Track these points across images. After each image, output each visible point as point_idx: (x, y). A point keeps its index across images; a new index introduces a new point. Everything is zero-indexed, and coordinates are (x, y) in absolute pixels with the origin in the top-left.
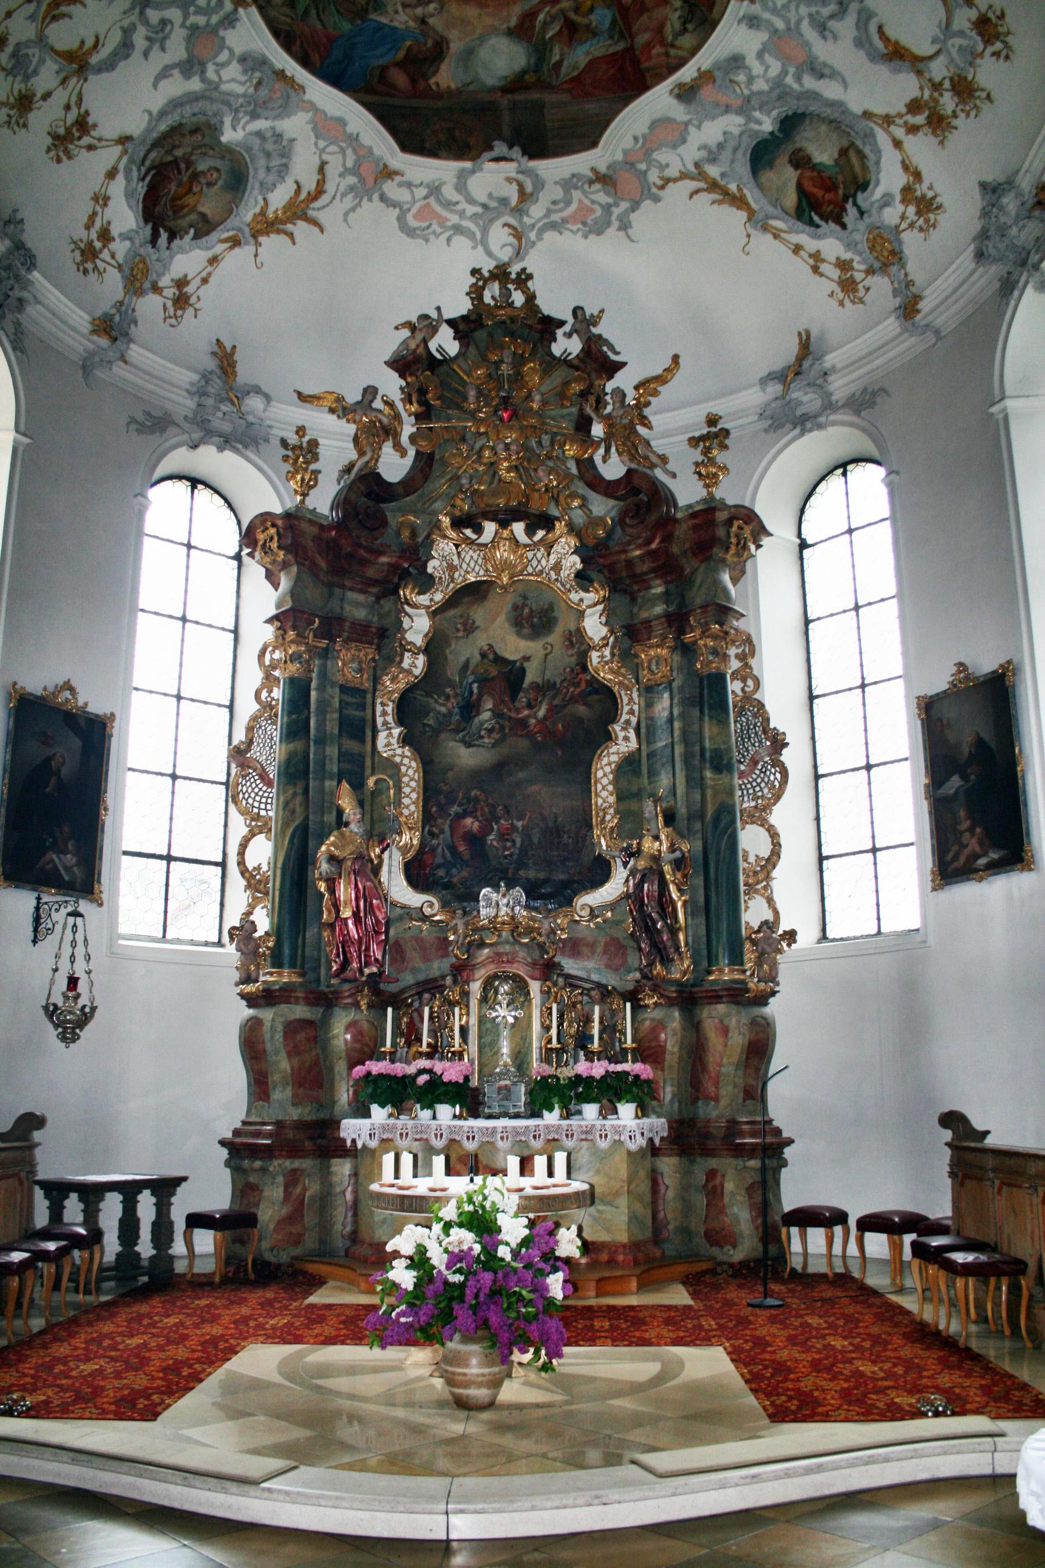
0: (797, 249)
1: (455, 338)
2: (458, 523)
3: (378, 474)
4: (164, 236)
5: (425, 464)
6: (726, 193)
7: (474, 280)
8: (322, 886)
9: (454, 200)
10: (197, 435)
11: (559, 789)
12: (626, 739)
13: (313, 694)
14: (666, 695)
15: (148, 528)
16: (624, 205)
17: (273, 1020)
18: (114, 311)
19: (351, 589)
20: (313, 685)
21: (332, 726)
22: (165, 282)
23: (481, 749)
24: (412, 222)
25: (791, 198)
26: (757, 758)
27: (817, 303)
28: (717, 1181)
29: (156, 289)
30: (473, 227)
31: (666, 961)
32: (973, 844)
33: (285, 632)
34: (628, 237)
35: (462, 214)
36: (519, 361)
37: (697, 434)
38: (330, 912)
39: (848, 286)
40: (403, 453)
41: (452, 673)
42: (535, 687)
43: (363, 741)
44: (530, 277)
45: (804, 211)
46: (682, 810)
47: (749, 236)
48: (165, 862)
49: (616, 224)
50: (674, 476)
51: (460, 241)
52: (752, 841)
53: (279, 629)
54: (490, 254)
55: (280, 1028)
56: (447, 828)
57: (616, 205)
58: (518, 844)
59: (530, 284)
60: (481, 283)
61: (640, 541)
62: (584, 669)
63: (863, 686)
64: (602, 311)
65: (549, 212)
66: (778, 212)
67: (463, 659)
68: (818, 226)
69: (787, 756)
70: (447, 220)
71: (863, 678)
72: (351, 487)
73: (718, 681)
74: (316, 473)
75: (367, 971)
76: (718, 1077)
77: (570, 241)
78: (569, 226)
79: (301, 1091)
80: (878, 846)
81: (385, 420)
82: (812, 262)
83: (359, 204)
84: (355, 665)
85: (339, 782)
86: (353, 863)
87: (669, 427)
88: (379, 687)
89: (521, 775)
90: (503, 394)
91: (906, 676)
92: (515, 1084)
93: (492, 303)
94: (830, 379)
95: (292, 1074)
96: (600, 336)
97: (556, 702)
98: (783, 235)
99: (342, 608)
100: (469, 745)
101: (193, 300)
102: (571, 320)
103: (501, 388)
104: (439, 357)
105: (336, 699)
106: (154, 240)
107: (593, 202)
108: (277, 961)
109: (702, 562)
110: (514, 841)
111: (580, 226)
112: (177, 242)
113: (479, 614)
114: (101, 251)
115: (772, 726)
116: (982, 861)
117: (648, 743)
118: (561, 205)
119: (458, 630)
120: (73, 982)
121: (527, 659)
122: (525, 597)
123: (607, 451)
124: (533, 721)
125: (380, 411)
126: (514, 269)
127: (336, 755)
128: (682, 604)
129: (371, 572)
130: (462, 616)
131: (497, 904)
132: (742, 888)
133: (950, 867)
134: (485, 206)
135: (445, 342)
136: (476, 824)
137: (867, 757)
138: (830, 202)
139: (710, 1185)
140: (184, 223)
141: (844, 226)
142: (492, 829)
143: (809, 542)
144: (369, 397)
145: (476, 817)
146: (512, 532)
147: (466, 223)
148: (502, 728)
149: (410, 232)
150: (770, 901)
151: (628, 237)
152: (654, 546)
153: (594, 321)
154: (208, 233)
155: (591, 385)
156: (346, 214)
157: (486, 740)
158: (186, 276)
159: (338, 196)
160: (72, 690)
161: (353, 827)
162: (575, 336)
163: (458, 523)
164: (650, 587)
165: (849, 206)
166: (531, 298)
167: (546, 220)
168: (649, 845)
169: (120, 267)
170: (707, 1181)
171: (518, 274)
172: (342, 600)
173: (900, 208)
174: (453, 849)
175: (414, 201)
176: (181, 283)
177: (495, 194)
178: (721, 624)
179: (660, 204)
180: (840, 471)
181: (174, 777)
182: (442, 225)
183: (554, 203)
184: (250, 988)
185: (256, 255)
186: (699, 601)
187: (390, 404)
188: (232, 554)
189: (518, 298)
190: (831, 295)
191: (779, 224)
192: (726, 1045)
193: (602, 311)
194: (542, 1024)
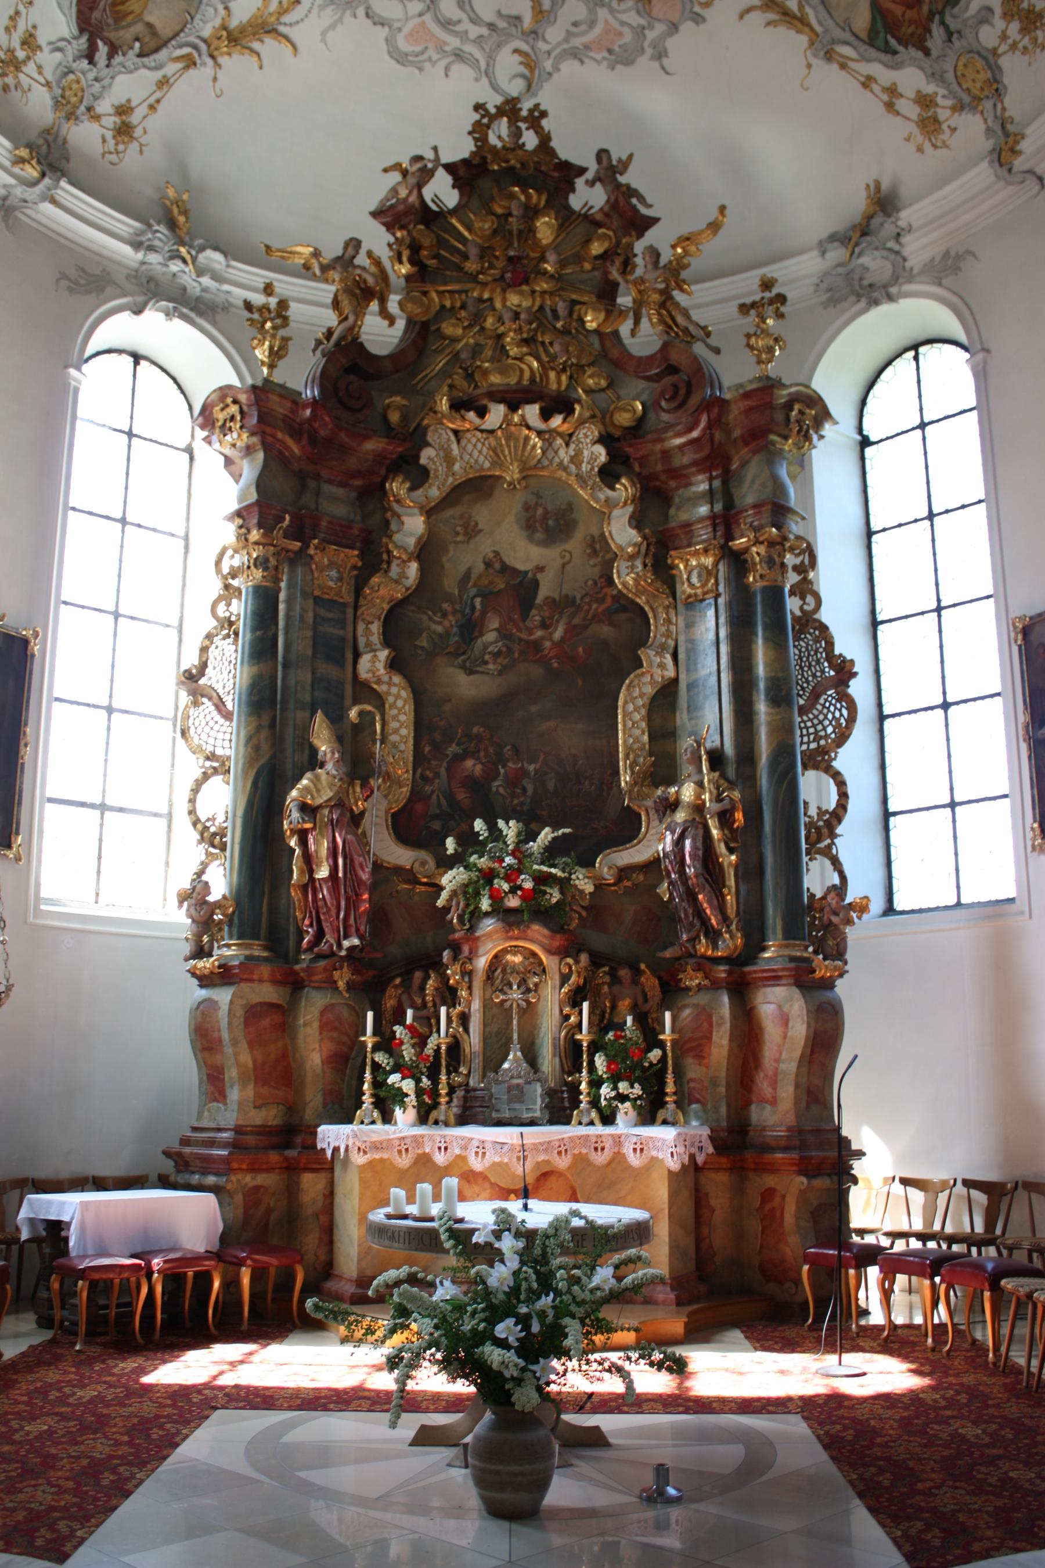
0: (867, 83)
1: (454, 187)
2: (458, 406)
3: (361, 344)
4: (103, 49)
5: (422, 333)
6: (786, 13)
7: (477, 117)
8: (293, 843)
9: (455, 19)
10: (140, 299)
11: (580, 726)
12: (662, 666)
13: (282, 607)
14: (711, 613)
15: (81, 412)
16: (660, 28)
17: (231, 1002)
18: (41, 141)
19: (329, 482)
20: (282, 596)
21: (304, 646)
22: (104, 107)
23: (487, 678)
24: (403, 45)
25: (862, 19)
26: (819, 689)
27: (890, 149)
28: (776, 1202)
30: (477, 53)
31: (713, 936)
33: (249, 531)
34: (663, 68)
35: (464, 35)
36: (531, 213)
37: (748, 300)
38: (301, 872)
39: (930, 125)
40: (391, 320)
41: (450, 584)
42: (551, 602)
43: (341, 664)
44: (544, 114)
45: (877, 33)
46: (729, 749)
47: (809, 66)
48: (98, 812)
49: (649, 51)
50: (717, 351)
51: (460, 70)
52: (814, 791)
53: (241, 527)
54: (495, 87)
55: (240, 1013)
56: (443, 771)
57: (651, 27)
58: (529, 793)
59: (544, 122)
60: (485, 121)
61: (679, 428)
62: (610, 582)
63: (939, 609)
64: (631, 156)
65: (569, 35)
66: (847, 35)
67: (463, 569)
68: (895, 53)
70: (445, 43)
71: (939, 600)
72: (329, 356)
73: (774, 596)
74: (285, 340)
75: (346, 944)
76: (776, 1074)
77: (593, 75)
78: (592, 54)
79: (264, 1090)
80: (957, 799)
81: (370, 281)
82: (885, 98)
83: (340, 20)
84: (334, 573)
85: (313, 713)
86: (331, 812)
88: (362, 601)
89: (534, 708)
90: (512, 253)
91: (1001, 594)
92: (529, 1083)
93: (499, 145)
94: (904, 240)
95: (255, 1069)
96: (628, 186)
97: (575, 621)
98: (851, 64)
99: (317, 503)
100: (470, 672)
101: (138, 132)
102: (593, 167)
103: (510, 246)
104: (434, 207)
106: (90, 56)
107: (622, 23)
109: (754, 452)
110: (524, 789)
111: (606, 54)
112: (118, 59)
113: (482, 514)
114: (25, 62)
115: (837, 652)
117: (688, 670)
118: (584, 27)
119: (457, 534)
121: (541, 569)
122: (538, 496)
123: (637, 322)
124: (547, 644)
125: (364, 269)
126: (526, 106)
127: (309, 681)
128: (729, 504)
129: (352, 463)
130: (461, 517)
132: (804, 846)
134: (491, 26)
135: (442, 191)
136: (479, 767)
137: (944, 693)
138: (910, 22)
139: (767, 1207)
140: (127, 35)
141: (927, 52)
142: (498, 774)
143: (873, 439)
144: (350, 251)
145: (478, 759)
146: (523, 417)
147: (468, 48)
148: (510, 650)
149: (401, 58)
151: (663, 68)
152: (695, 434)
153: (624, 165)
154: (157, 50)
155: (618, 244)
156: (324, 33)
157: (491, 666)
158: (129, 101)
159: (315, 10)
161: (329, 766)
162: (598, 185)
163: (458, 406)
164: (690, 484)
165: (935, 27)
166: (545, 140)
167: (566, 46)
168: (688, 792)
169: (48, 84)
170: (763, 1202)
171: (531, 111)
172: (318, 494)
173: (999, 24)
174: (450, 797)
175: (407, 19)
176: (123, 110)
177: (504, 12)
178: (779, 528)
179: (702, 26)
180: (912, 353)
181: (110, 710)
182: (441, 49)
183: (575, 24)
184: (205, 964)
185: (215, 79)
186: (750, 500)
187: (377, 262)
188: (183, 446)
189: (530, 140)
190: (908, 139)
191: (847, 51)
192: (785, 1036)
193: (631, 156)
194: (561, 1011)
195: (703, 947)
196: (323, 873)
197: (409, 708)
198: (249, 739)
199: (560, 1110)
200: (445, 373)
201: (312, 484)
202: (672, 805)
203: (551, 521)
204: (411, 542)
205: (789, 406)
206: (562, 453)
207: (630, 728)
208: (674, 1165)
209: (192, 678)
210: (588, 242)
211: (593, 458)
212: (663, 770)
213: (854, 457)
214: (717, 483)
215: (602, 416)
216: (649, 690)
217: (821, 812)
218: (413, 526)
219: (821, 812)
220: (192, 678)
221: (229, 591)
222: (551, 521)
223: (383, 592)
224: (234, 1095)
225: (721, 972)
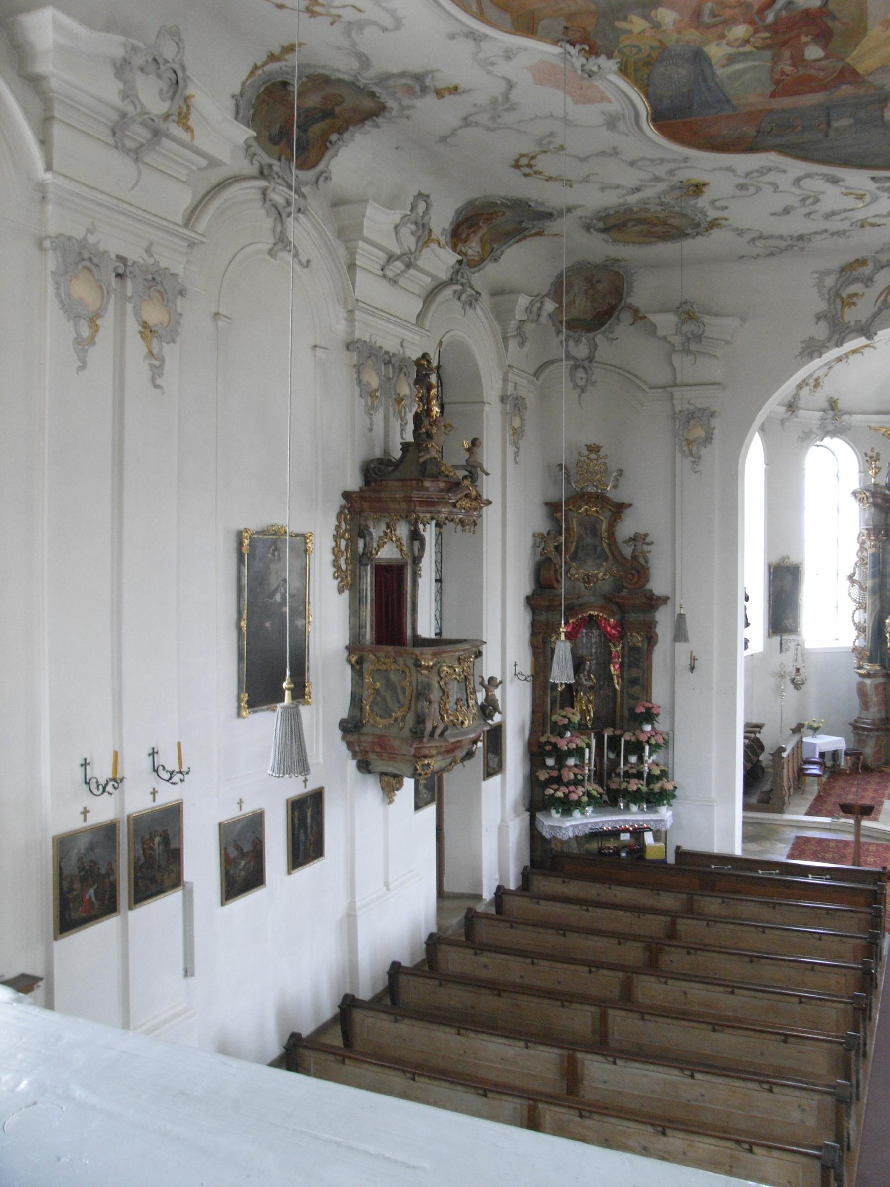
29: (807, 384)
108: (871, 660)
120: (798, 670)
160: (788, 558)
198: (873, 603)
209: (851, 578)
220: (851, 578)
221: (862, 548)
224: (872, 710)
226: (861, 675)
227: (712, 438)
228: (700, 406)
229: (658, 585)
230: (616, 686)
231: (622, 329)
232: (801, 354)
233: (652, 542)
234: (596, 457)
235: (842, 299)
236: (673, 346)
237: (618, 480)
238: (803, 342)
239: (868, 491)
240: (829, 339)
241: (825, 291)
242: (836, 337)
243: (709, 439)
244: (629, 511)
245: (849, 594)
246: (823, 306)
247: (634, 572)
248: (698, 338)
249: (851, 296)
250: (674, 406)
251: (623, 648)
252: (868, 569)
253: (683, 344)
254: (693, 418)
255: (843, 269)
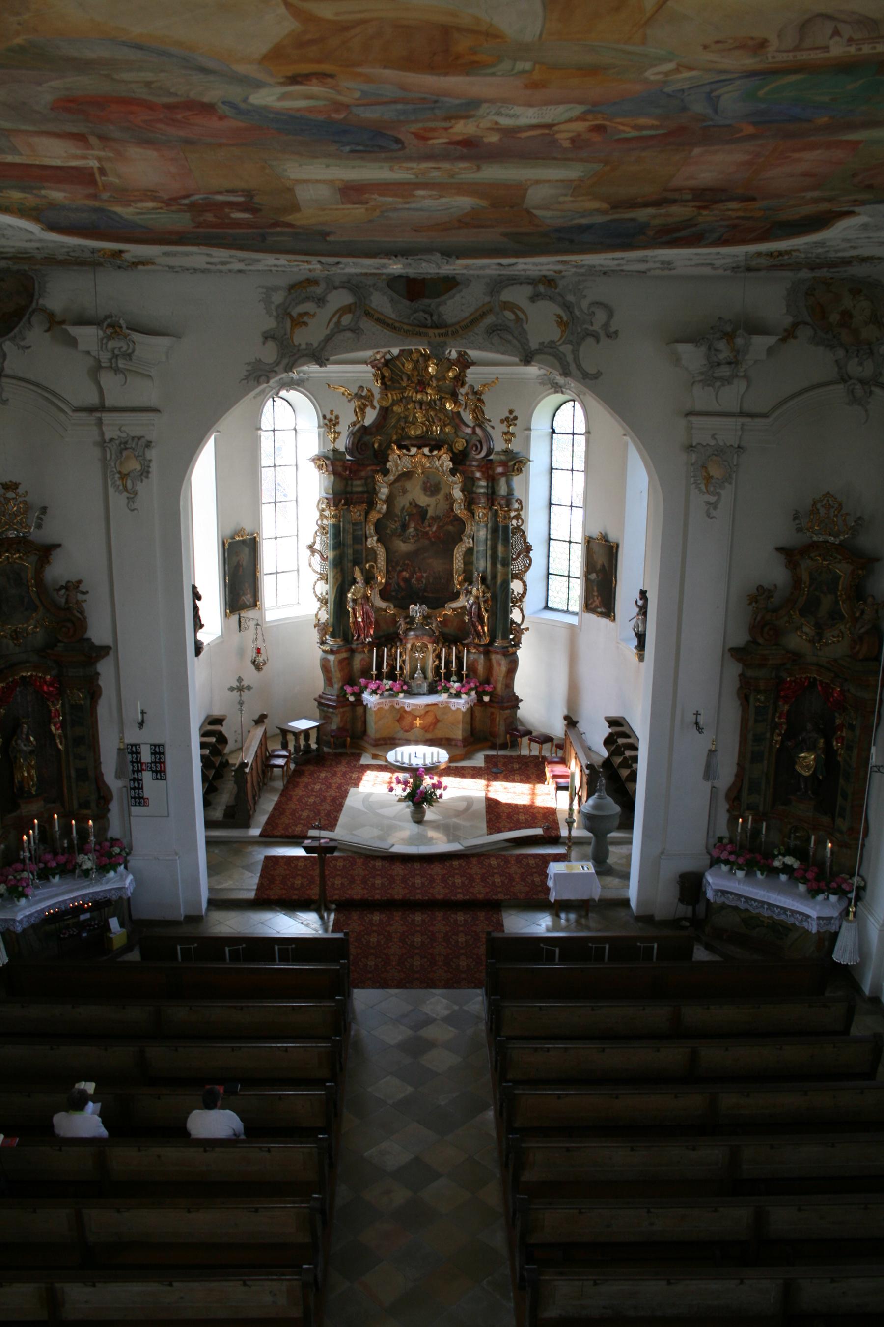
5: (385, 412)
12: (469, 543)
31: (479, 636)
32: (597, 602)
36: (427, 358)
40: (374, 408)
41: (397, 511)
42: (432, 518)
43: (362, 544)
46: (489, 578)
50: (493, 427)
52: (516, 586)
62: (452, 510)
67: (402, 505)
69: (532, 554)
72: (353, 434)
73: (506, 528)
87: (494, 412)
100: (404, 542)
105: (349, 527)
108: (333, 636)
113: (408, 485)
116: (599, 610)
120: (259, 651)
121: (428, 506)
122: (428, 478)
131: (416, 610)
133: (588, 607)
150: (522, 610)
160: (242, 530)
168: (474, 591)
174: (398, 584)
195: (476, 641)
196: (360, 620)
197: (383, 550)
199: (432, 691)
200: (395, 426)
201: (349, 482)
202: (471, 593)
203: (433, 488)
204: (384, 497)
205: (515, 464)
206: (437, 463)
207: (458, 563)
208: (464, 709)
209: (311, 547)
210: (448, 371)
211: (447, 466)
212: (469, 580)
213: (549, 438)
214: (490, 484)
215: (451, 450)
216: (464, 549)
217: (518, 594)
218: (384, 491)
219: (518, 594)
220: (311, 547)
221: (322, 516)
222: (433, 488)
223: (374, 516)
225: (481, 649)
226: (324, 651)
227: (148, 472)
228: (132, 434)
229: (98, 633)
230: (60, 746)
231: (36, 335)
232: (247, 378)
233: (87, 592)
234: (14, 496)
235: (291, 317)
236: (99, 361)
237: (41, 519)
238: (249, 364)
239: (327, 458)
240: (277, 364)
241: (273, 307)
242: (285, 361)
243: (145, 472)
244: (59, 550)
245: (310, 565)
246: (270, 324)
247: (69, 625)
248: (128, 356)
249: (301, 315)
250: (102, 434)
251: (63, 706)
252: (329, 539)
253: (110, 360)
254: (126, 449)
255: (292, 287)
